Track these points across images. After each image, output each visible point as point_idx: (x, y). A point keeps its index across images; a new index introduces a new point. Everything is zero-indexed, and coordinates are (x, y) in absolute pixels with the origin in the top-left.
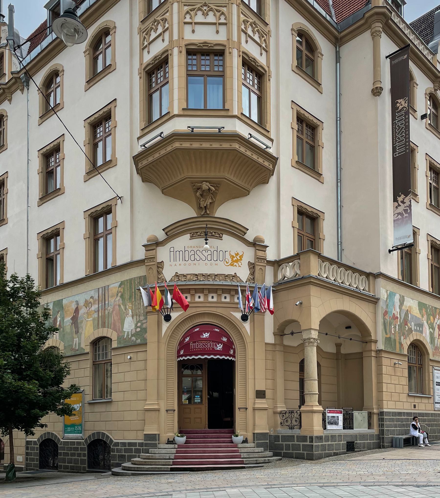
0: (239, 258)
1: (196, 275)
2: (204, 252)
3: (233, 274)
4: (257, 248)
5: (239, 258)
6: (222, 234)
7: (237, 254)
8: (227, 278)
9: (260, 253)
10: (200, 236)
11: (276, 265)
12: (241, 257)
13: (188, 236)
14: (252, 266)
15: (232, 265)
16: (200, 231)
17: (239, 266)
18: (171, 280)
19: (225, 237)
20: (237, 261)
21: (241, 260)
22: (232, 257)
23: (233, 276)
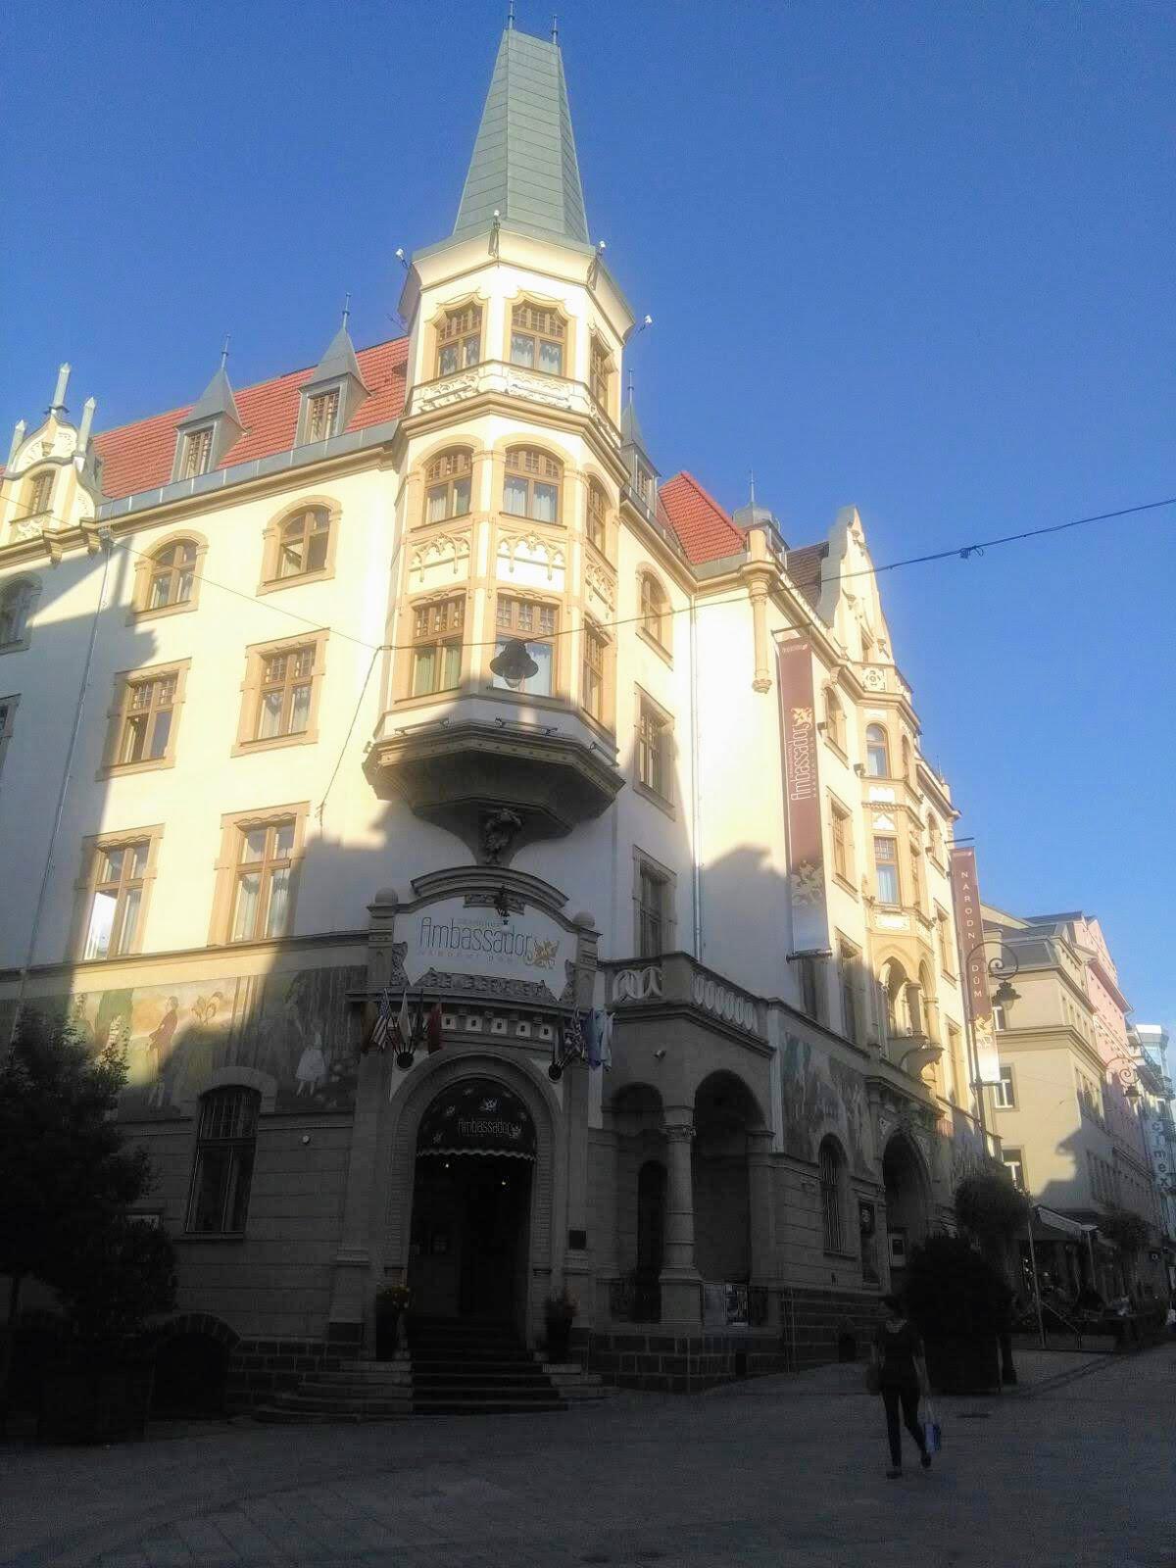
0: (550, 953)
1: (471, 978)
2: (488, 936)
3: (539, 981)
4: (586, 936)
5: (550, 953)
6: (524, 904)
7: (548, 945)
8: (527, 988)
9: (588, 947)
10: (484, 904)
11: (611, 973)
12: (554, 951)
13: (461, 901)
14: (572, 970)
15: (538, 964)
16: (486, 893)
17: (551, 968)
18: (420, 983)
19: (528, 908)
20: (547, 958)
21: (554, 955)
22: (539, 949)
23: (540, 987)
